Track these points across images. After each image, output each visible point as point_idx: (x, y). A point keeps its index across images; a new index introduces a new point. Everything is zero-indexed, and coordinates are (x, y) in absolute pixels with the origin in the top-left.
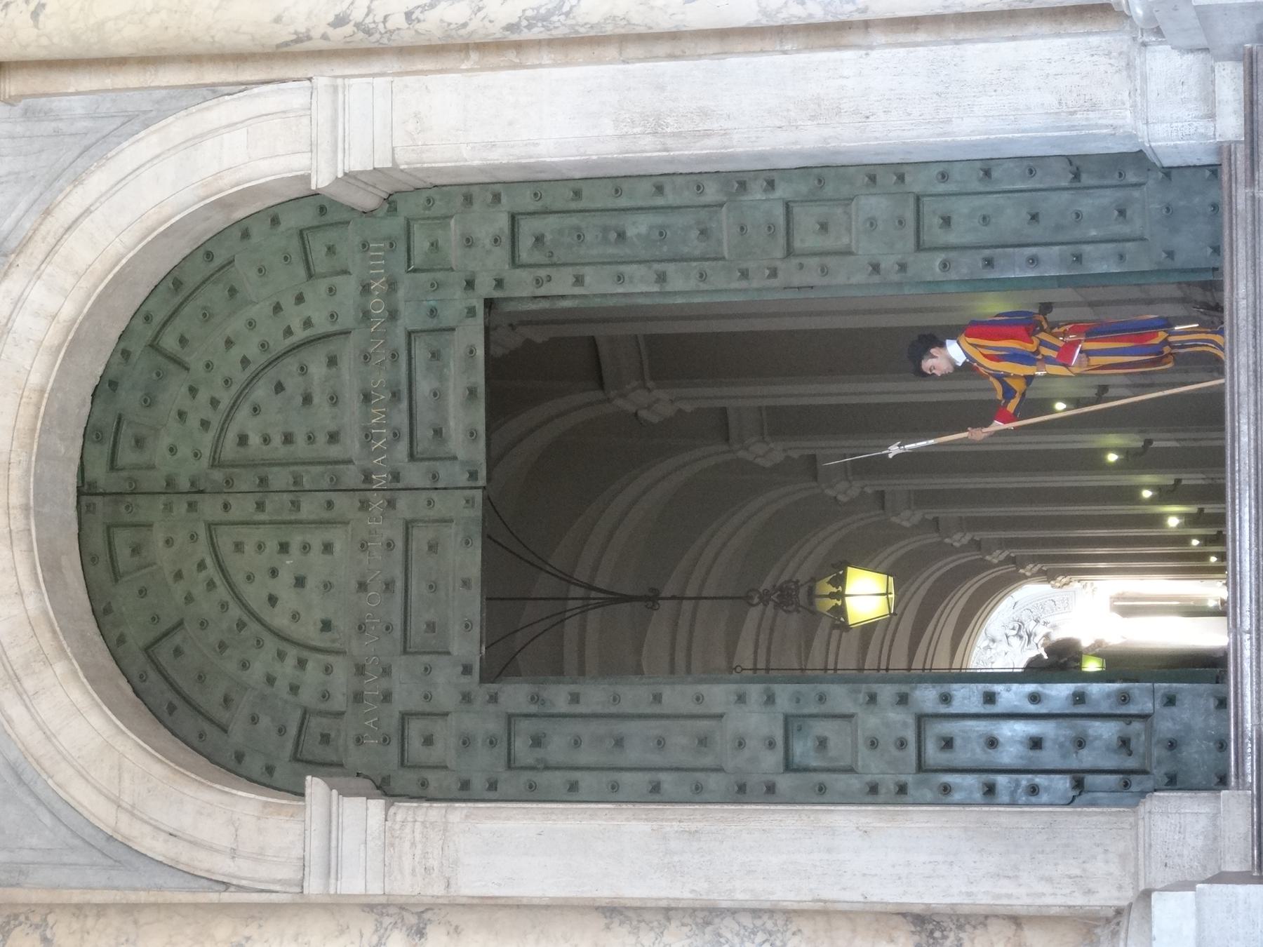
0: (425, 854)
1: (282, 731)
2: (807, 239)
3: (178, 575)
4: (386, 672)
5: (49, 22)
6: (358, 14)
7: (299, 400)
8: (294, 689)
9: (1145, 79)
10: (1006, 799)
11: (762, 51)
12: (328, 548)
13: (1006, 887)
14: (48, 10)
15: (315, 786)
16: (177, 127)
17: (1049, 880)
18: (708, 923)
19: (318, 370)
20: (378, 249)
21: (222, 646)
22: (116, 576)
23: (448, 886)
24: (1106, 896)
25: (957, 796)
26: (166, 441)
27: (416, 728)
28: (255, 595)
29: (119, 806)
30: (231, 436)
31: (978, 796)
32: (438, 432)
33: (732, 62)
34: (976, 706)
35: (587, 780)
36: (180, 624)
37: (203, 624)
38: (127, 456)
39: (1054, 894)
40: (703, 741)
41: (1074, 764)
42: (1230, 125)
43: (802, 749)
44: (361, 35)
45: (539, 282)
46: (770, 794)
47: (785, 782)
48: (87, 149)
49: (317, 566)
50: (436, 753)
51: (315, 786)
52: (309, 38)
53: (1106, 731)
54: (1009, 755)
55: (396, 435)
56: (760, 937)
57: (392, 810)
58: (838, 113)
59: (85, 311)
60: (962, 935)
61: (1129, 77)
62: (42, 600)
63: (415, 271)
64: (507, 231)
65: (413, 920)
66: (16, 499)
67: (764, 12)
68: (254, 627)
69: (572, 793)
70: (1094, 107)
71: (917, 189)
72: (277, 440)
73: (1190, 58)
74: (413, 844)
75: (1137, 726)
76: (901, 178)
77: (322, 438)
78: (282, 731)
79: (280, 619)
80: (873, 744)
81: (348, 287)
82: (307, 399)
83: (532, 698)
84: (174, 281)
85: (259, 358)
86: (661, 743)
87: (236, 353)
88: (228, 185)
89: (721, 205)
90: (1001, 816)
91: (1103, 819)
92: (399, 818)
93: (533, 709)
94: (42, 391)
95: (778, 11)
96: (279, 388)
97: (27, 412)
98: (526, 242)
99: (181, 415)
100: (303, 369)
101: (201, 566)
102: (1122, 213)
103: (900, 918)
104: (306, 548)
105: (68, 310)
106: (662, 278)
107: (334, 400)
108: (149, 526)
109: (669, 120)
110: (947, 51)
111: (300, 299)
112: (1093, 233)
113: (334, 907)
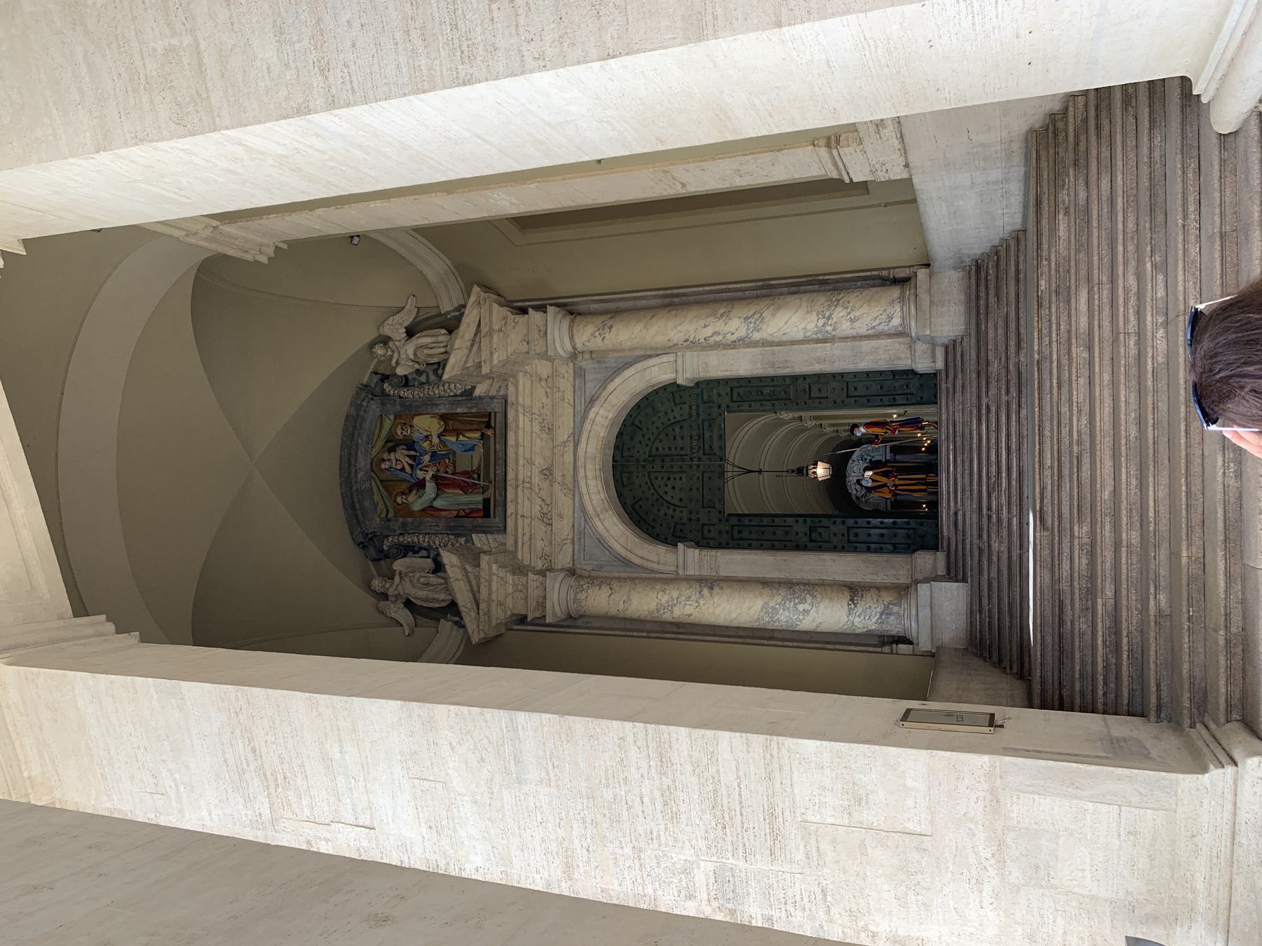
13: (874, 577)
15: (680, 545)
16: (639, 366)
19: (677, 430)
22: (624, 486)
28: (661, 492)
35: (754, 543)
38: (626, 454)
40: (787, 533)
46: (805, 548)
49: (678, 484)
50: (711, 535)
51: (680, 545)
54: (874, 538)
69: (749, 547)
79: (668, 498)
81: (686, 407)
84: (638, 406)
88: (654, 381)
98: (735, 395)
105: (610, 416)
113: (688, 579)
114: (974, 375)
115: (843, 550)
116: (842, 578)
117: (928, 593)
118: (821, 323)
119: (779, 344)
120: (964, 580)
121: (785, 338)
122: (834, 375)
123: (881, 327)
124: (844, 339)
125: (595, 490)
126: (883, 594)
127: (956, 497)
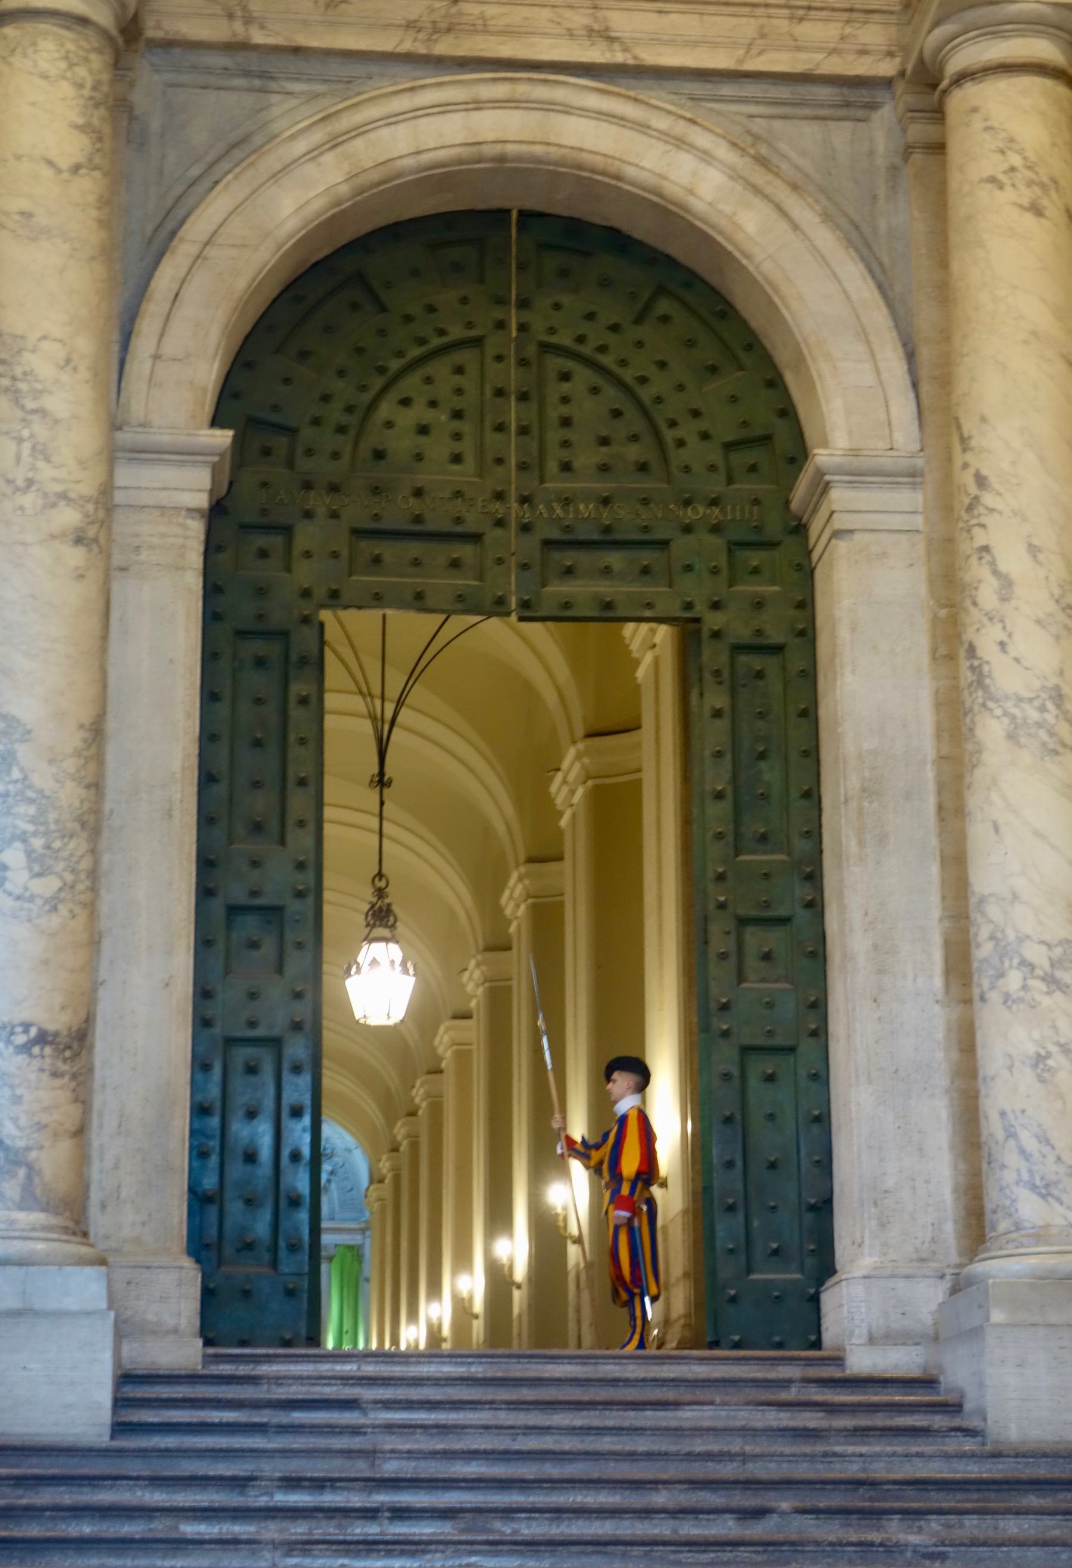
0: (152, 547)
1: (276, 408)
2: (755, 939)
3: (431, 309)
4: (334, 515)
5: (985, 194)
6: (988, 499)
7: (604, 433)
8: (316, 422)
9: (908, 1277)
10: (196, 1126)
11: (943, 898)
12: (457, 459)
14: (997, 193)
15: (224, 437)
16: (878, 317)
17: (116, 1167)
18: (83, 825)
19: (634, 452)
20: (751, 513)
21: (359, 351)
23: (123, 569)
24: (98, 1221)
25: (199, 1077)
26: (565, 299)
27: (276, 541)
28: (412, 384)
29: (206, 244)
30: (569, 364)
31: (199, 1098)
32: (569, 571)
33: (934, 869)
34: (289, 1097)
36: (383, 309)
37: (382, 332)
39: (101, 1172)
40: (257, 828)
41: (229, 1194)
42: (862, 1360)
43: (250, 926)
44: (967, 501)
45: (717, 673)
46: (205, 892)
47: (217, 906)
48: (857, 228)
49: (438, 448)
51: (224, 437)
52: (965, 450)
53: (261, 1227)
55: (567, 529)
56: (69, 877)
57: (197, 515)
58: (880, 972)
59: (697, 223)
60: (67, 1078)
61: (911, 1261)
62: (412, 172)
63: (730, 550)
64: (766, 642)
65: (91, 533)
66: (511, 148)
67: (982, 901)
68: (378, 382)
69: (209, 696)
70: (883, 1225)
71: (802, 1049)
72: (565, 410)
73: (929, 1321)
74: (163, 535)
75: (266, 1257)
76: (814, 1034)
77: (565, 455)
78: (276, 408)
79: (386, 409)
80: (253, 995)
81: (716, 486)
82: (605, 441)
83: (304, 657)
85: (646, 394)
86: (257, 785)
87: (652, 371)
88: (820, 368)
89: (789, 854)
90: (181, 1122)
91: (176, 1221)
92: (189, 522)
93: (294, 658)
94: (618, 178)
95: (983, 914)
96: (617, 414)
97: (598, 161)
98: (756, 662)
99: (591, 316)
100: (635, 438)
101: (442, 332)
102: (776, 1252)
103: (83, 1015)
104: (457, 436)
105: (697, 205)
106: (719, 796)
107: (604, 468)
108: (482, 280)
109: (875, 805)
110: (941, 1080)
111: (705, 436)
112: (756, 1223)
114: (853, 1470)
115: (202, 1022)
116: (104, 1010)
117: (71, 1303)
118: (1036, 954)
119: (953, 810)
120: (120, 1428)
121: (978, 832)
122: (819, 1006)
123: (1011, 1158)
124: (966, 1043)
125: (424, 133)
126: (65, 1147)
127: (409, 1405)
